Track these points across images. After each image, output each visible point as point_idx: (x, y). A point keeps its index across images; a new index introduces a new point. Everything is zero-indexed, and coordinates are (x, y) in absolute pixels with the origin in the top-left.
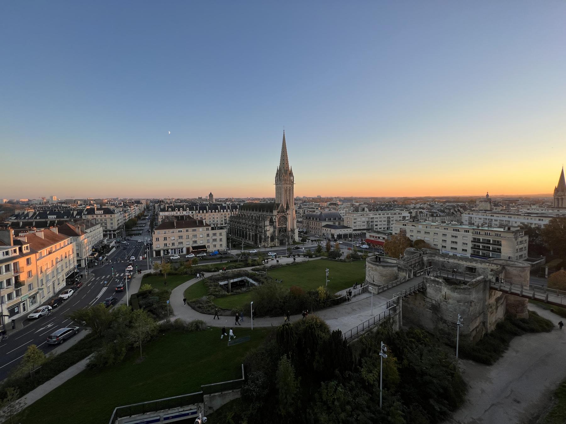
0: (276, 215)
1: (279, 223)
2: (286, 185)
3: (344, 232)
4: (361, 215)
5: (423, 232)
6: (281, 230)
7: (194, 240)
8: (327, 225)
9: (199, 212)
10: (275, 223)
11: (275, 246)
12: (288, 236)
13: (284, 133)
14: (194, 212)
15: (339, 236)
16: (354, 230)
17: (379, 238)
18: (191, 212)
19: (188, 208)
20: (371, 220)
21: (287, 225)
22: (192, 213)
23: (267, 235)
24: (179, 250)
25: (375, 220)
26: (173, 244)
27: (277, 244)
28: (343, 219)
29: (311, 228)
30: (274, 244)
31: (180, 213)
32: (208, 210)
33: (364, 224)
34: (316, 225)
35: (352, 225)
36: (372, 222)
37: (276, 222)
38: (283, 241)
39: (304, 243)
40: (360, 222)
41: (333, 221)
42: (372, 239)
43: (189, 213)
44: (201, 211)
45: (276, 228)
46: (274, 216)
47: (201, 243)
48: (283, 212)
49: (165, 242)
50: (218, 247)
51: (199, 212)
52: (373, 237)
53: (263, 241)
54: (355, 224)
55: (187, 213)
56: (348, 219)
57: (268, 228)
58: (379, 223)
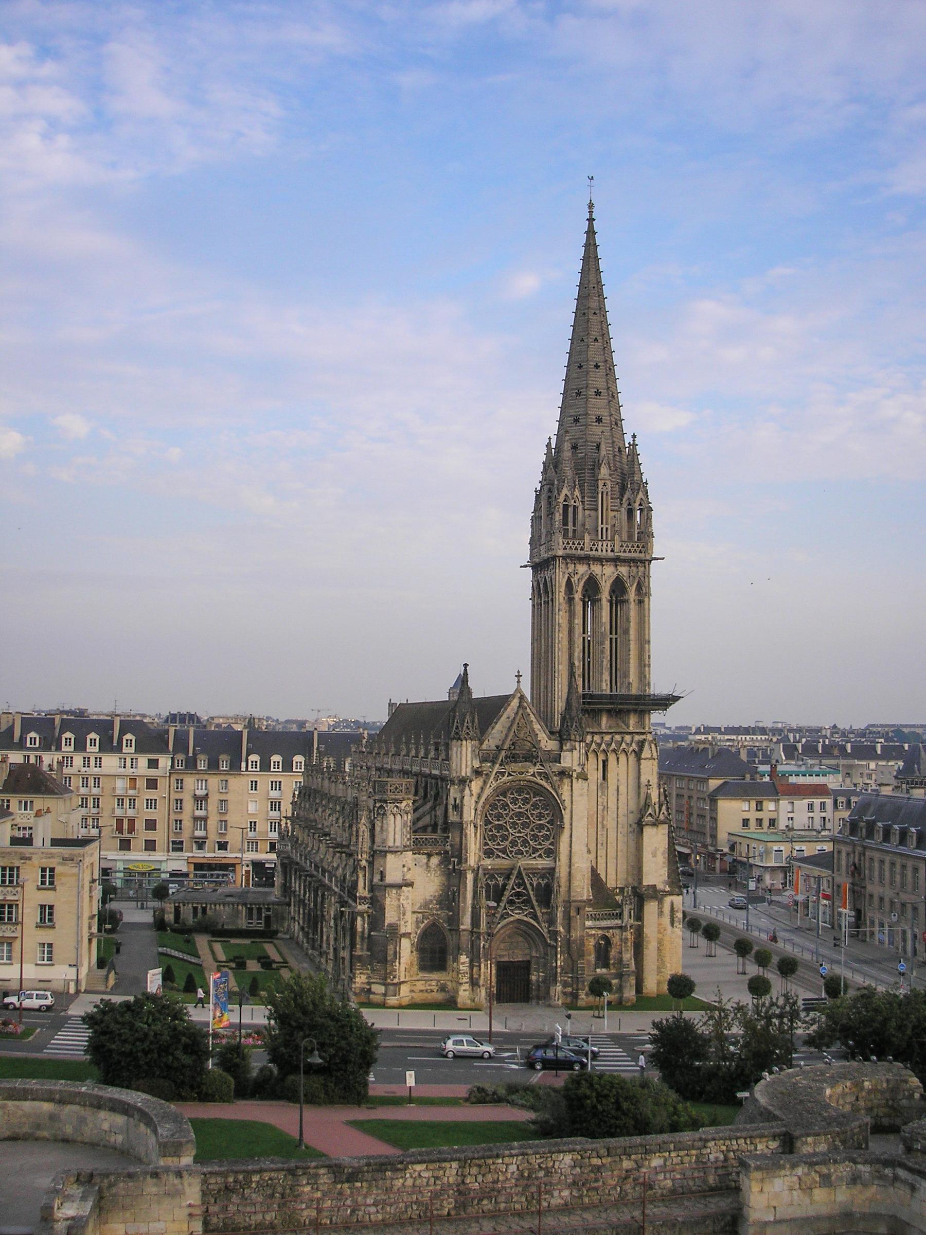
0: (466, 771)
1: (493, 838)
2: (582, 569)
6: (504, 886)
9: (191, 764)
10: (454, 836)
11: (450, 1004)
12: (568, 942)
13: (591, 220)
14: (165, 762)
18: (143, 761)
22: (153, 764)
34: (898, 878)
37: (460, 826)
38: (529, 974)
45: (461, 875)
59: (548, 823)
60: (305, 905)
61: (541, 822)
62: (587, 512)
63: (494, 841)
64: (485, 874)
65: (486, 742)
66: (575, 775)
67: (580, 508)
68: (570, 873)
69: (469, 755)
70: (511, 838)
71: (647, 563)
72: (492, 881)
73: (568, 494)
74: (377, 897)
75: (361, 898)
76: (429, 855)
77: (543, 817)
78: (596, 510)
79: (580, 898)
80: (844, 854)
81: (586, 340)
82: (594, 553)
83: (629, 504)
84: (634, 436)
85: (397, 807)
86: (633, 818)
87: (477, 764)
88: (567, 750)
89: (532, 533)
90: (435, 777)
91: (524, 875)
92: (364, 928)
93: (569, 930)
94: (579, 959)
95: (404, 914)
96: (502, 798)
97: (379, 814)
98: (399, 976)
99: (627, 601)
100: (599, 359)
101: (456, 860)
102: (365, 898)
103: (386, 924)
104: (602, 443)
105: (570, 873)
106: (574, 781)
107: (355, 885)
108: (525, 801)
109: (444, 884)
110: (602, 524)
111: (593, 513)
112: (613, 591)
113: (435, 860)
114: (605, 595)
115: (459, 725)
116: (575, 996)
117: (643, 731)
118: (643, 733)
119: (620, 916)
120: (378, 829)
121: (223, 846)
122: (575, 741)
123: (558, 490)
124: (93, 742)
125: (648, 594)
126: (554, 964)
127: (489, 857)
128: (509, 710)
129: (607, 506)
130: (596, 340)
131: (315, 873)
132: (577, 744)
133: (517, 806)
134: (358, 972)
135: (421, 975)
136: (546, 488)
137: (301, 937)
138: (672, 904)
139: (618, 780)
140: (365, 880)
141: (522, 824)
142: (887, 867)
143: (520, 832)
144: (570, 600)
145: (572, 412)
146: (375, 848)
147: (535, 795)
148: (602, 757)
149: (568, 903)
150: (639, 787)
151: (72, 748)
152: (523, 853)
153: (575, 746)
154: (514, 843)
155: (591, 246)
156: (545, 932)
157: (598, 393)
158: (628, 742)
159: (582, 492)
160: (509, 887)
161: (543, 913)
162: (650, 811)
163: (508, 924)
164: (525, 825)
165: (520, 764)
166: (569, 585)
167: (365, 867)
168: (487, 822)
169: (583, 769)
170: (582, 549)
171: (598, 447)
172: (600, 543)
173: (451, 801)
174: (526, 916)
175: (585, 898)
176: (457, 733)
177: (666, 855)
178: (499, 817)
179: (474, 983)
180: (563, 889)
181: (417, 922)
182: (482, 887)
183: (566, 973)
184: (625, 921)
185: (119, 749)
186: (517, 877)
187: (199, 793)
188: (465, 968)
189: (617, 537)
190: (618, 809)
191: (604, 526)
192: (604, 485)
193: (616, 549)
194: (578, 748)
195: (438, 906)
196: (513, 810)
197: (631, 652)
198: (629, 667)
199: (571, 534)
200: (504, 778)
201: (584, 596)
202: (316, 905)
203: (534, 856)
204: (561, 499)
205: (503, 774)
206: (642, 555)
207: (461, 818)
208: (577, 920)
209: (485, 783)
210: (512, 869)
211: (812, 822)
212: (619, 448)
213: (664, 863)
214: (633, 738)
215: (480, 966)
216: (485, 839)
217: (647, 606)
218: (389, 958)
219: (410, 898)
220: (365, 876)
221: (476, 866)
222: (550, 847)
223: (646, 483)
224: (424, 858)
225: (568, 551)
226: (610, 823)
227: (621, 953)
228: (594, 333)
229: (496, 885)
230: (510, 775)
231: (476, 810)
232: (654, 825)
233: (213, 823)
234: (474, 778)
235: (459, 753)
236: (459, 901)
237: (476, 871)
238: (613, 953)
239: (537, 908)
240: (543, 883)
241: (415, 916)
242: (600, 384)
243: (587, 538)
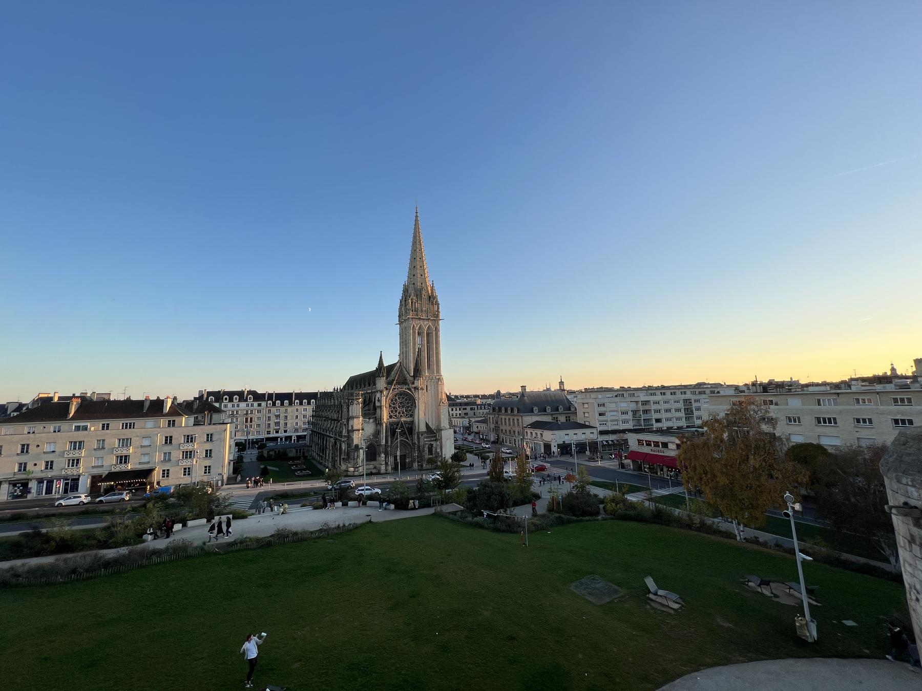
3: (575, 437)
4: (616, 396)
5: (808, 421)
7: (119, 453)
8: (537, 421)
9: (274, 404)
10: (378, 411)
11: (378, 473)
12: (419, 447)
14: (263, 404)
15: (565, 449)
16: (602, 433)
17: (665, 445)
18: (256, 404)
19: (250, 396)
20: (641, 408)
21: (413, 418)
22: (259, 405)
24: (67, 484)
25: (653, 407)
26: (50, 465)
27: (383, 468)
28: (576, 409)
29: (504, 431)
30: (375, 468)
31: (233, 406)
32: (293, 400)
33: (625, 417)
34: (511, 423)
35: (595, 420)
36: (646, 412)
37: (380, 407)
38: (405, 459)
39: (462, 463)
40: (615, 413)
41: (552, 414)
42: (646, 450)
43: (252, 405)
44: (278, 402)
46: (377, 392)
47: (144, 463)
48: (404, 382)
49: (23, 458)
50: (198, 476)
51: (274, 404)
52: (647, 445)
53: (343, 459)
54: (602, 418)
55: (248, 405)
56: (586, 406)
57: (357, 423)
58: (663, 415)
75: (344, 436)
80: (491, 418)
90: (369, 393)
93: (419, 443)
107: (341, 432)
108: (403, 398)
116: (422, 466)
121: (285, 431)
124: (236, 399)
131: (323, 433)
136: (404, 298)
137: (318, 458)
142: (507, 420)
149: (418, 433)
151: (228, 401)
154: (399, 413)
155: (416, 220)
156: (411, 444)
164: (403, 407)
168: (390, 406)
173: (377, 399)
178: (394, 404)
179: (386, 464)
180: (417, 428)
185: (246, 400)
187: (276, 414)
199: (414, 310)
205: (395, 389)
208: (422, 438)
218: (355, 457)
224: (367, 420)
225: (413, 317)
227: (436, 449)
229: (393, 428)
233: (282, 422)
238: (434, 450)
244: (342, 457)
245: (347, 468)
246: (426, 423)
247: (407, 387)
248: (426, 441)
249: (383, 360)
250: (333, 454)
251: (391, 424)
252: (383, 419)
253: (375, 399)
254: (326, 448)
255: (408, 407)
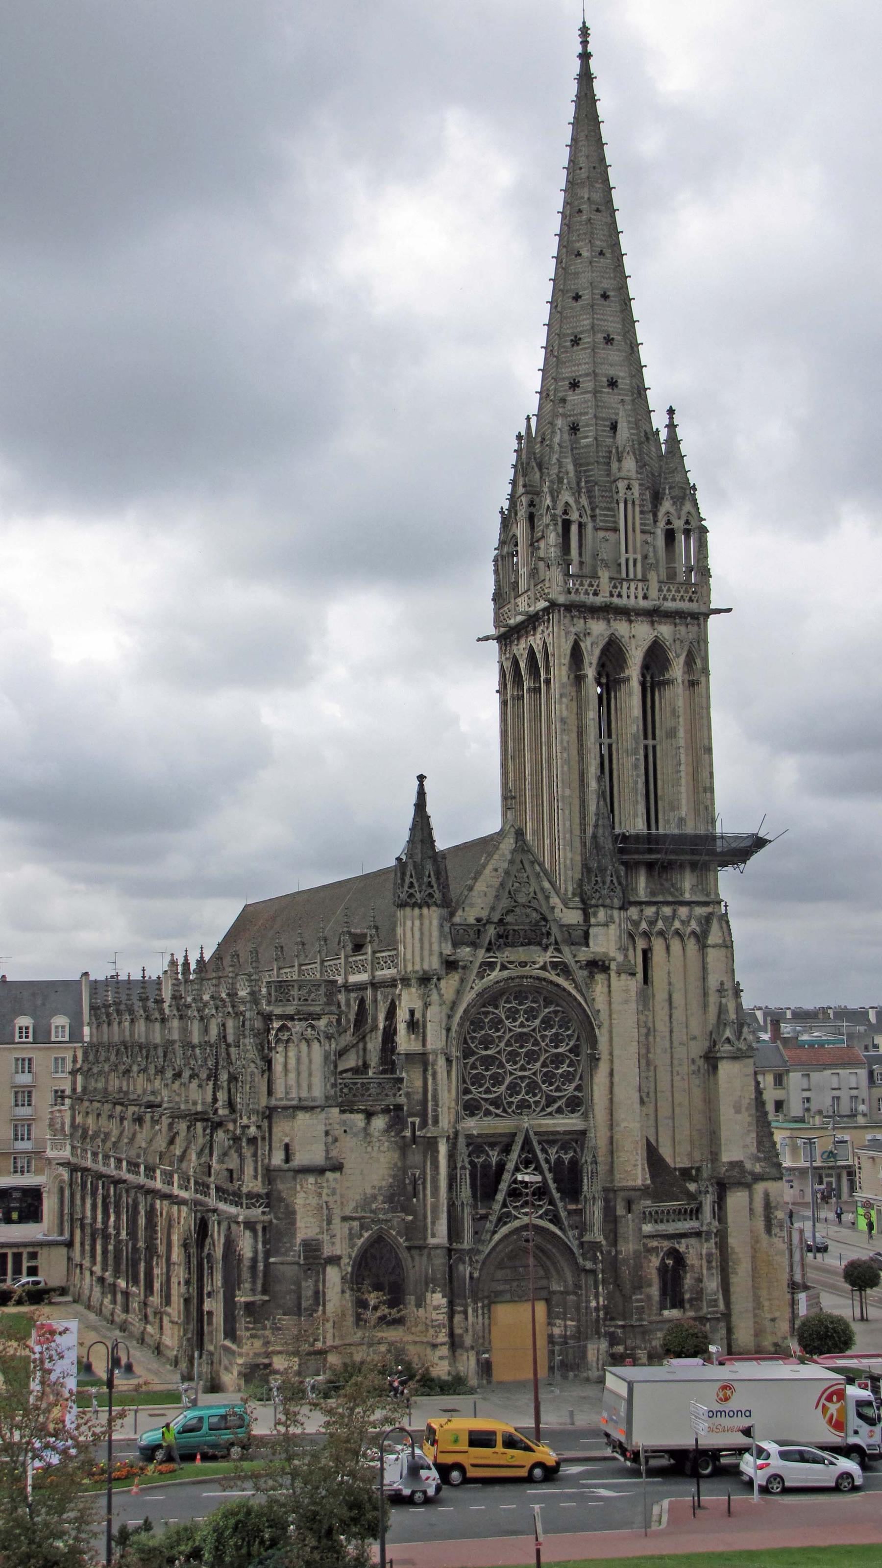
1: (477, 1080)
10: (412, 1078)
12: (613, 1264)
21: (585, 1116)
23: (293, 1223)
45: (431, 1144)
53: (249, 1307)
59: (570, 1051)
60: (106, 1237)
61: (560, 1050)
62: (601, 534)
63: (481, 1086)
64: (468, 1145)
65: (460, 912)
66: (613, 966)
67: (590, 526)
68: (612, 1138)
69: (435, 934)
70: (508, 1080)
71: (702, 619)
72: (478, 1157)
73: (571, 501)
74: (279, 1192)
75: (250, 1195)
76: (369, 1115)
77: (562, 1041)
78: (616, 530)
79: (631, 1183)
81: (585, 254)
82: (615, 600)
83: (669, 522)
84: (671, 412)
85: (313, 1027)
86: (698, 1048)
87: (448, 949)
88: (598, 925)
89: (497, 582)
90: (360, 987)
91: (535, 1144)
92: (256, 1252)
93: (614, 1243)
94: (634, 1294)
95: (329, 1222)
96: (491, 1009)
97: (278, 1041)
98: (324, 1338)
99: (669, 682)
100: (607, 284)
101: (417, 1120)
102: (258, 1196)
103: (298, 1241)
104: (620, 421)
105: (612, 1138)
106: (613, 974)
108: (531, 1014)
109: (395, 1165)
110: (627, 552)
111: (610, 535)
112: (646, 667)
113: (379, 1123)
114: (634, 671)
115: (414, 881)
117: (707, 899)
118: (706, 904)
119: (696, 1213)
120: (278, 1068)
122: (612, 908)
123: (552, 497)
125: (706, 671)
126: (593, 1304)
127: (472, 1115)
128: (496, 857)
129: (634, 524)
130: (601, 253)
132: (616, 913)
133: (517, 1023)
134: (248, 1334)
135: (360, 1334)
138: (767, 1195)
139: (670, 984)
140: (256, 1162)
141: (527, 1054)
143: (523, 1069)
144: (579, 679)
145: (567, 372)
146: (273, 1102)
147: (548, 1002)
148: (641, 944)
149: (609, 1193)
150: (705, 994)
152: (529, 1107)
153: (612, 917)
156: (574, 1245)
157: (609, 340)
158: (684, 917)
159: (590, 497)
160: (510, 1166)
161: (570, 1213)
162: (728, 1033)
163: (511, 1233)
164: (532, 1057)
165: (521, 949)
166: (576, 655)
167: (255, 1138)
168: (467, 1053)
169: (626, 956)
170: (596, 594)
171: (614, 427)
172: (625, 585)
173: (402, 1015)
174: (540, 1217)
175: (639, 1182)
176: (411, 896)
177: (753, 1111)
178: (487, 1043)
180: (602, 1168)
181: (351, 1237)
182: (463, 1168)
183: (612, 1319)
184: (705, 1222)
186: (523, 1149)
188: (441, 1317)
189: (653, 577)
190: (671, 1031)
191: (631, 556)
192: (629, 488)
193: (653, 593)
194: (617, 920)
195: (386, 1206)
196: (510, 1030)
197: (683, 768)
198: (680, 793)
200: (495, 973)
201: (599, 674)
202: (132, 1233)
203: (549, 1110)
204: (559, 511)
205: (491, 966)
206: (694, 607)
207: (424, 1045)
209: (462, 980)
210: (515, 1134)
211: (838, 1104)
212: (646, 433)
213: (750, 1124)
214: (691, 911)
215: (465, 1313)
216: (464, 1082)
217: (704, 691)
218: (304, 1304)
219: (338, 1191)
220: (255, 1155)
221: (451, 1131)
222: (576, 1093)
223: (695, 490)
224: (359, 1119)
225: (573, 597)
226: (660, 1058)
228: (598, 243)
229: (486, 1166)
230: (504, 968)
231: (448, 1030)
232: (735, 1058)
234: (444, 972)
235: (416, 929)
236: (425, 1195)
237: (453, 1141)
238: (688, 1281)
239: (560, 1205)
240: (567, 1157)
241: (346, 1225)
242: (613, 326)
243: (604, 575)
244: (241, 1298)
245: (268, 1355)
246: (649, 1143)
247: (547, 957)
248: (651, 1237)
249: (434, 822)
250: (188, 1282)
251: (477, 1145)
252: (436, 1122)
253: (391, 1014)
254: (151, 1249)
255: (558, 1060)
